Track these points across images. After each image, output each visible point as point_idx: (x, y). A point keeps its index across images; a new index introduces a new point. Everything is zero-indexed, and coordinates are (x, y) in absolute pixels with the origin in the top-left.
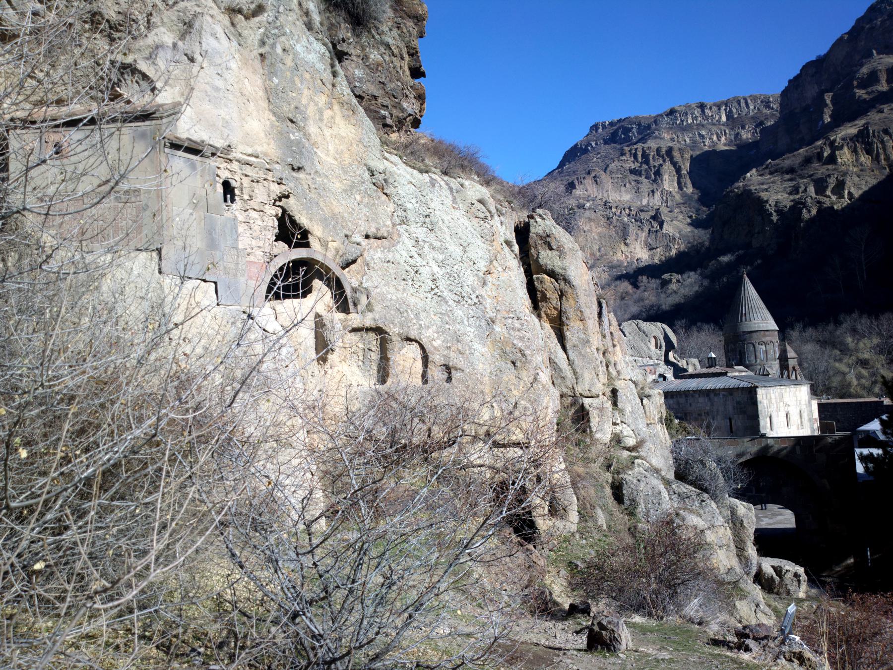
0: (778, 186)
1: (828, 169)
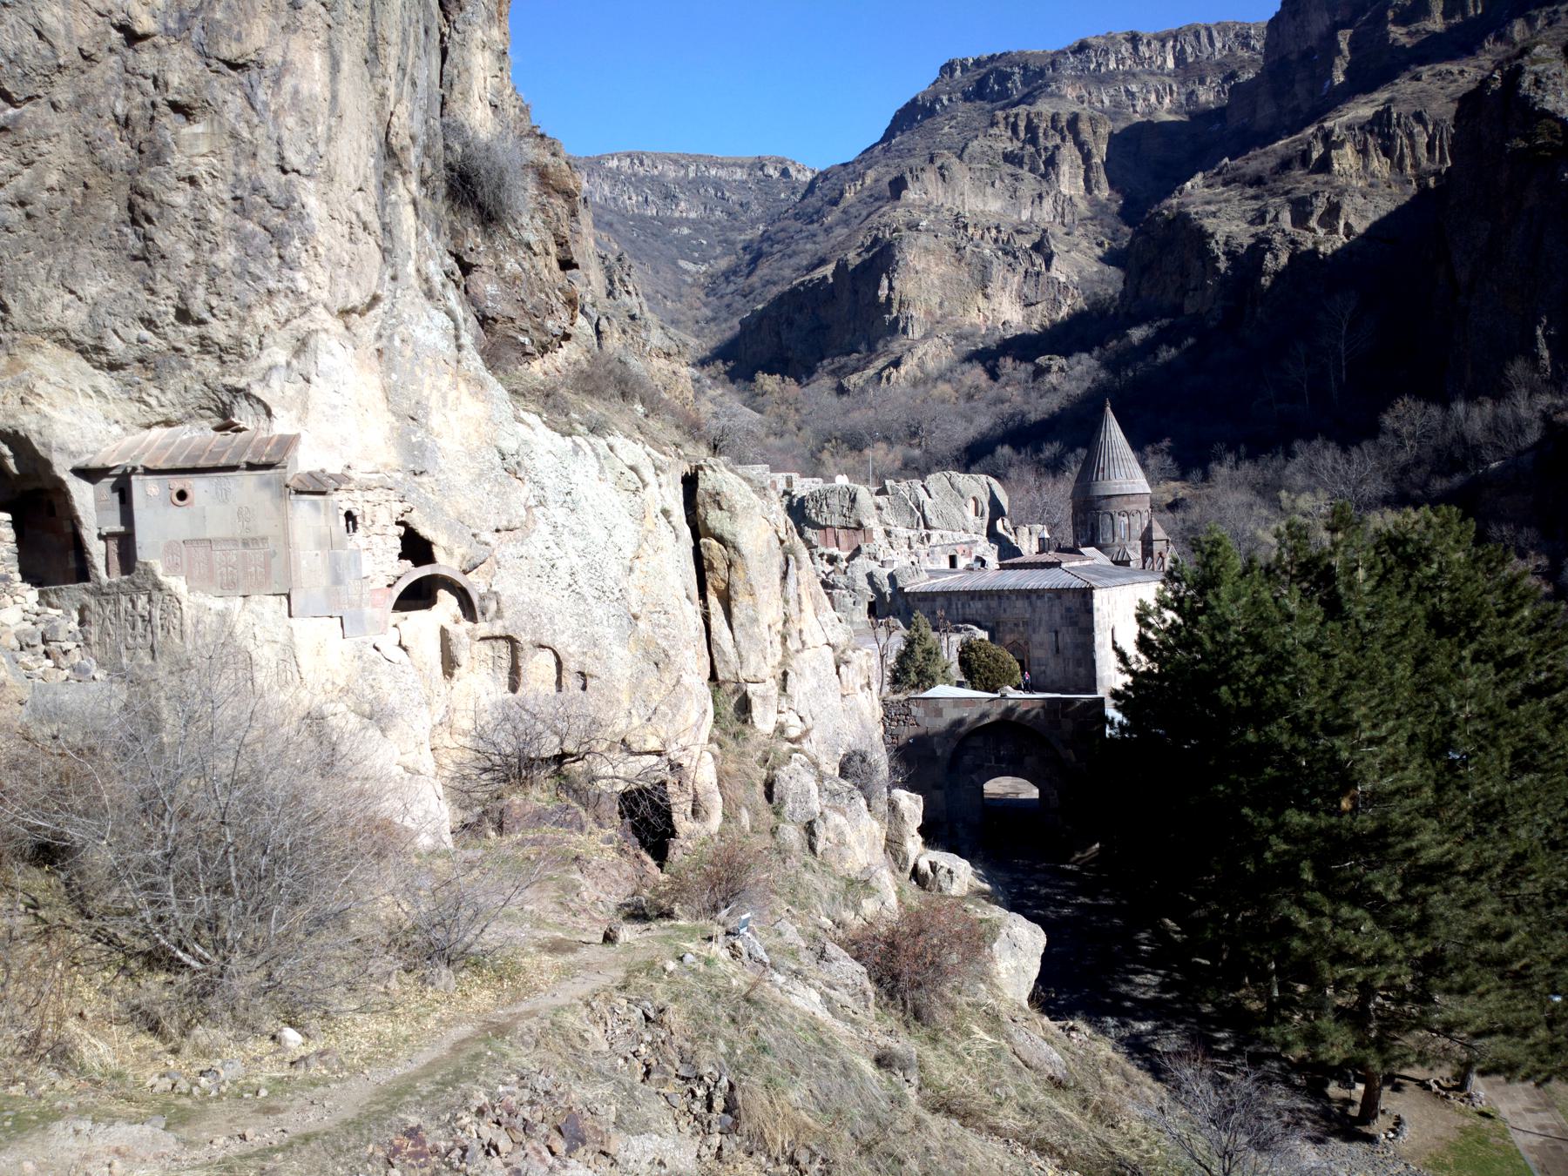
0: (1234, 209)
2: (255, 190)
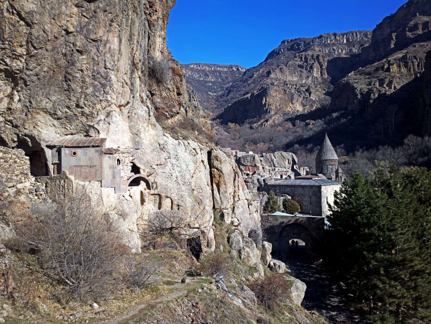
1: (386, 75)
2: (98, 73)
